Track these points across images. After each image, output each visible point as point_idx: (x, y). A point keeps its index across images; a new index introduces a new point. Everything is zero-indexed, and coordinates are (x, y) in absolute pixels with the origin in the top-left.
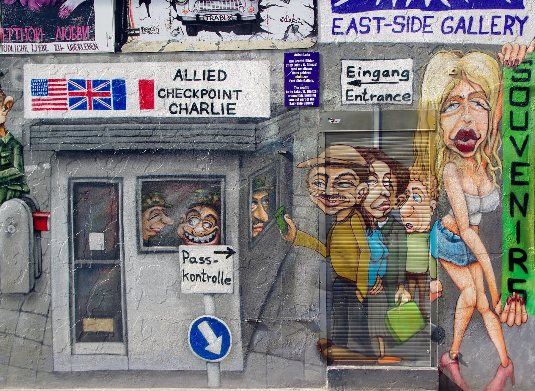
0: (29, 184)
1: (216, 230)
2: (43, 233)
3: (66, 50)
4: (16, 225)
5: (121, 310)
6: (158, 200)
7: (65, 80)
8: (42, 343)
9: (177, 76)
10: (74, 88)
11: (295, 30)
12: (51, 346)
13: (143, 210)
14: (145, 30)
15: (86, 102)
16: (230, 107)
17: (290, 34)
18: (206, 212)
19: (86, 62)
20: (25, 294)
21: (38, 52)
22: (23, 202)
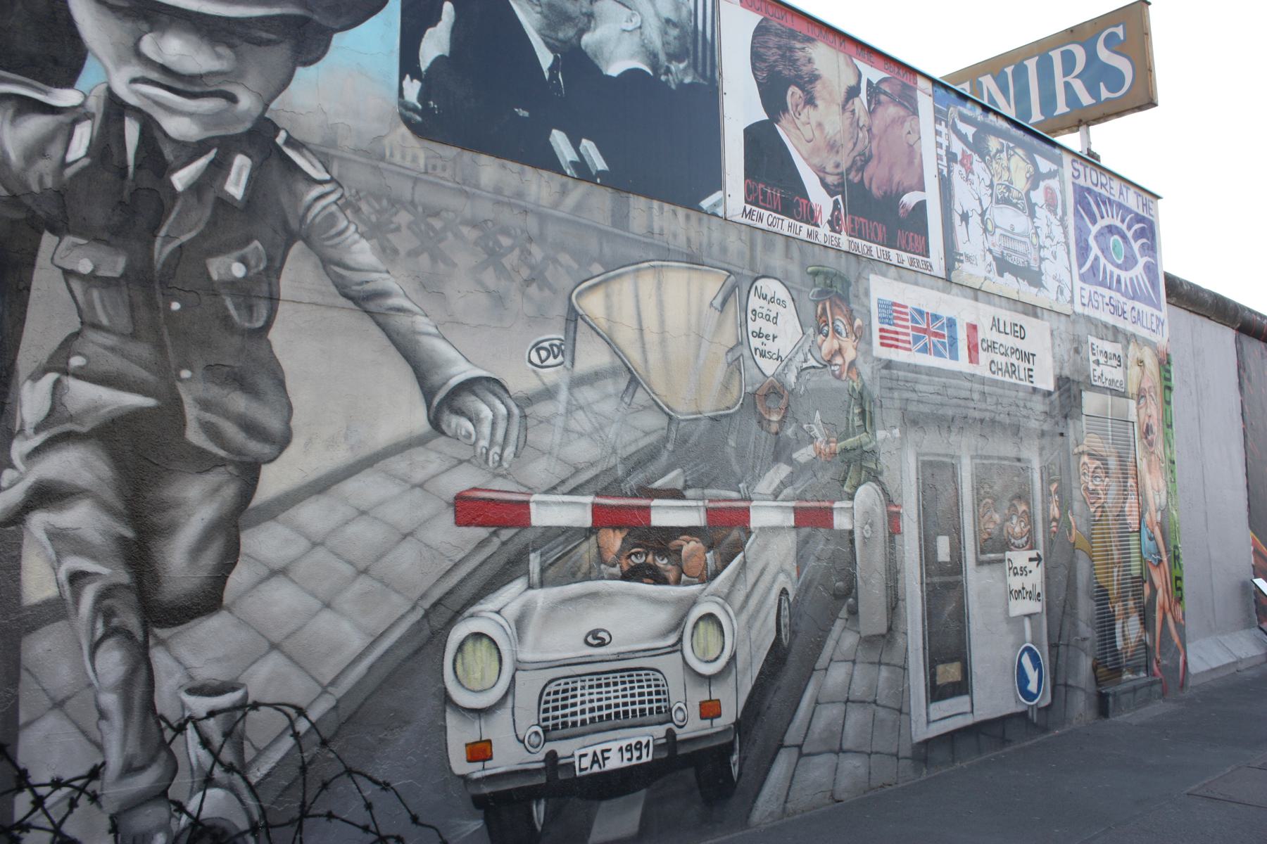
0: (882, 459)
1: (1029, 531)
2: (897, 537)
3: (906, 264)
4: (871, 525)
5: (965, 648)
6: (988, 490)
7: (905, 307)
8: (900, 711)
9: (993, 325)
10: (917, 323)
11: (1062, 293)
12: (909, 714)
13: (978, 505)
14: (969, 258)
15: (926, 344)
16: (1031, 373)
17: (1059, 296)
18: (1022, 507)
19: (924, 286)
20: (883, 636)
21: (882, 260)
22: (876, 487)
